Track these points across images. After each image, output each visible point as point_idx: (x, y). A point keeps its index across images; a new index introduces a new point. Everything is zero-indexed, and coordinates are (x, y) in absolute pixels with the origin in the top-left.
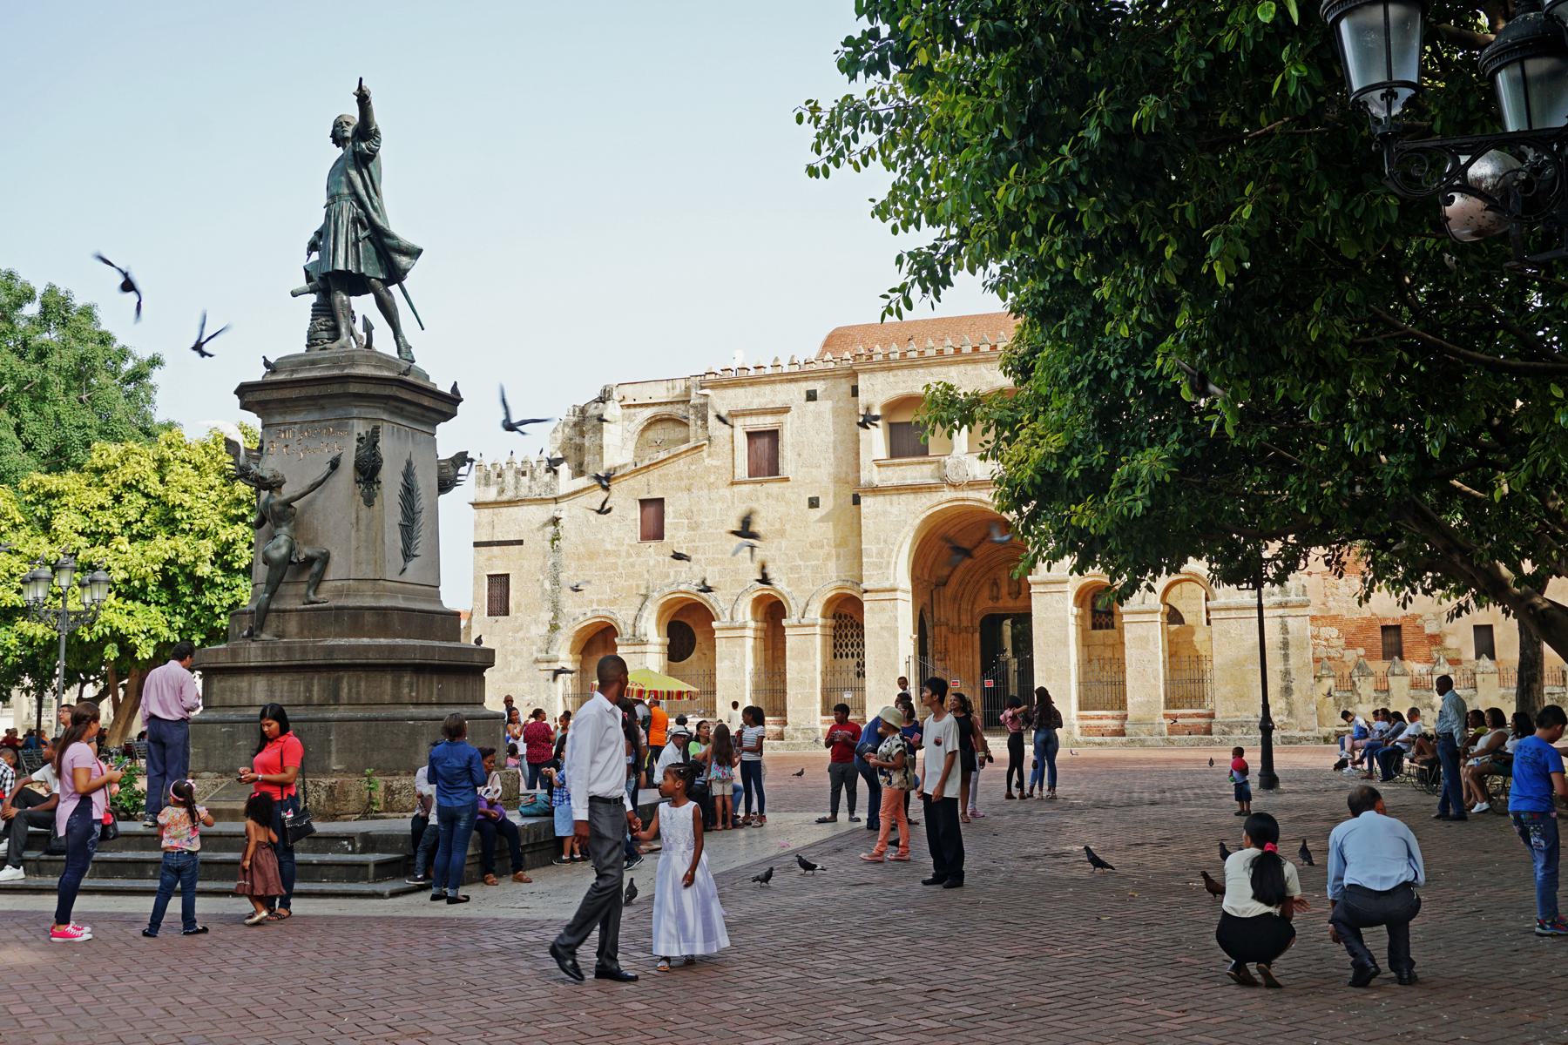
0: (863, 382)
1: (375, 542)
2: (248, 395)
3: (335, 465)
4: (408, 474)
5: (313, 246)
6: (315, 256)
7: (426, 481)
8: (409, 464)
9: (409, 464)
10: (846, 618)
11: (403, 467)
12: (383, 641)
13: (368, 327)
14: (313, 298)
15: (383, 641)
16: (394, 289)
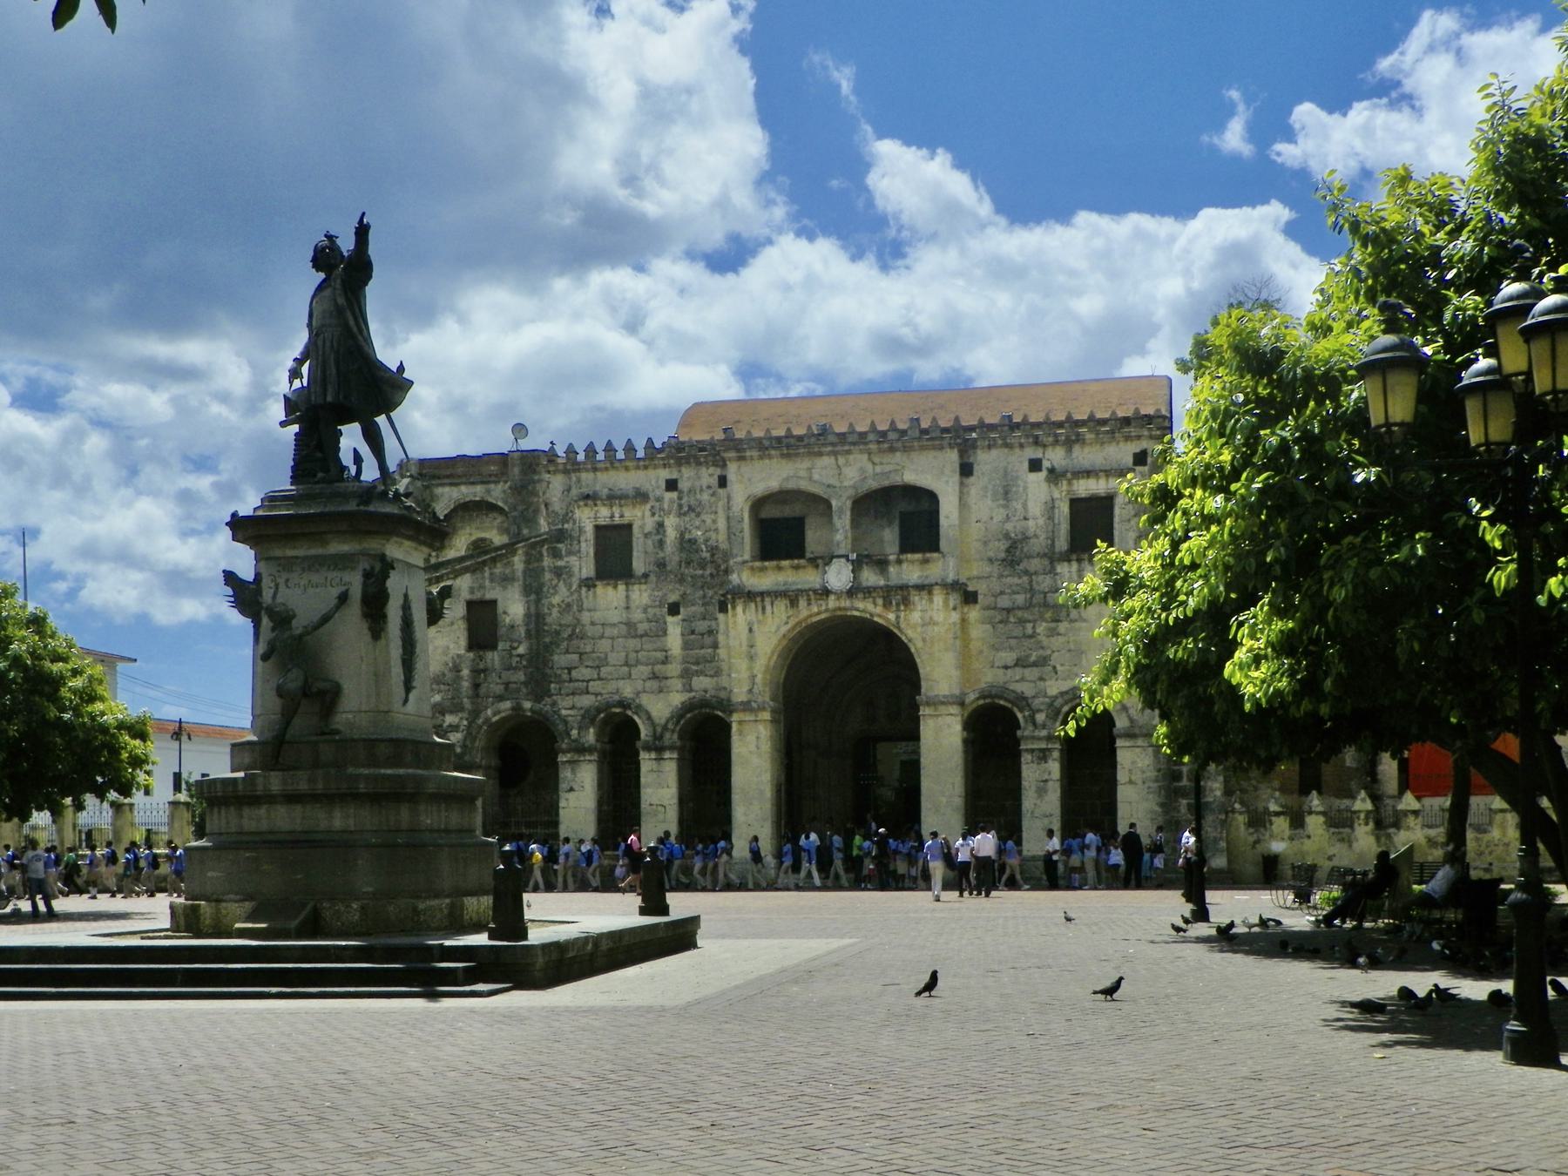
0: (732, 470)
1: (379, 677)
2: (241, 527)
3: (343, 598)
4: (406, 607)
5: (295, 374)
6: (297, 384)
7: (419, 614)
8: (406, 596)
9: (406, 596)
10: (704, 742)
11: (401, 601)
12: (402, 771)
13: (358, 459)
14: (295, 428)
15: (402, 771)
16: (381, 420)
